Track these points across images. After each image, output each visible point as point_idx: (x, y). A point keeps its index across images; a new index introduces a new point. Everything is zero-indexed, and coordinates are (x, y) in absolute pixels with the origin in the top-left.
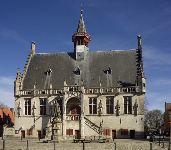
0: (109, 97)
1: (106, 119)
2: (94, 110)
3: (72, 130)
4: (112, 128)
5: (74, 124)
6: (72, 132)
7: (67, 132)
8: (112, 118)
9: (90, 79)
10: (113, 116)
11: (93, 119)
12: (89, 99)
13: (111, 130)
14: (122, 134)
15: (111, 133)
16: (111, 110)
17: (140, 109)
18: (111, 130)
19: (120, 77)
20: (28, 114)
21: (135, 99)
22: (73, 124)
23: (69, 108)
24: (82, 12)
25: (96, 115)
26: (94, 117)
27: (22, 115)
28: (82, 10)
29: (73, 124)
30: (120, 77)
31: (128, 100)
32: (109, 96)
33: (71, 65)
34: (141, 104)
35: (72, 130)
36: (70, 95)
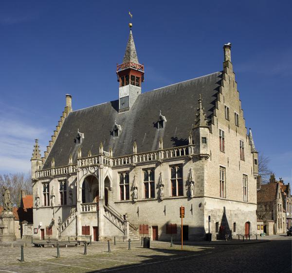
0: (147, 168)
1: (140, 206)
2: (127, 194)
3: (89, 227)
4: (151, 222)
5: (91, 218)
6: (89, 230)
7: (83, 230)
8: (153, 205)
9: (131, 141)
10: (154, 202)
11: (123, 209)
12: (118, 176)
13: (150, 225)
14: (167, 233)
15: (151, 231)
16: (153, 192)
17: (198, 187)
18: (150, 225)
19: (176, 130)
20: (177, 195)
21: (189, 168)
22: (90, 217)
23: (92, 192)
24: (131, 26)
25: (128, 201)
26: (126, 205)
27: (40, 206)
28: (131, 24)
29: (90, 217)
30: (176, 130)
31: (177, 171)
32: (146, 167)
33: (110, 119)
34: (199, 176)
35: (89, 227)
36: (85, 172)
